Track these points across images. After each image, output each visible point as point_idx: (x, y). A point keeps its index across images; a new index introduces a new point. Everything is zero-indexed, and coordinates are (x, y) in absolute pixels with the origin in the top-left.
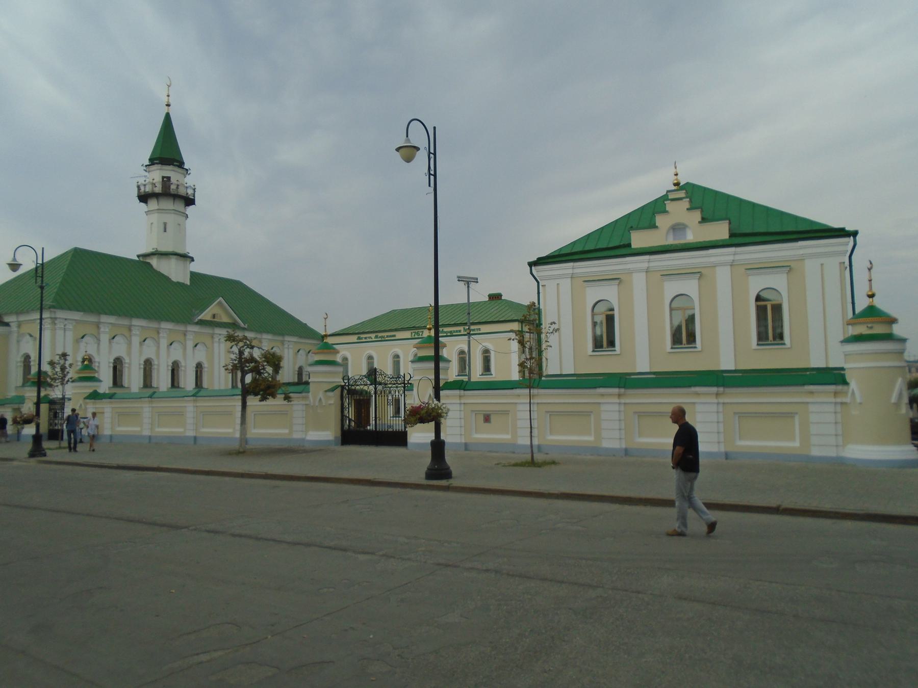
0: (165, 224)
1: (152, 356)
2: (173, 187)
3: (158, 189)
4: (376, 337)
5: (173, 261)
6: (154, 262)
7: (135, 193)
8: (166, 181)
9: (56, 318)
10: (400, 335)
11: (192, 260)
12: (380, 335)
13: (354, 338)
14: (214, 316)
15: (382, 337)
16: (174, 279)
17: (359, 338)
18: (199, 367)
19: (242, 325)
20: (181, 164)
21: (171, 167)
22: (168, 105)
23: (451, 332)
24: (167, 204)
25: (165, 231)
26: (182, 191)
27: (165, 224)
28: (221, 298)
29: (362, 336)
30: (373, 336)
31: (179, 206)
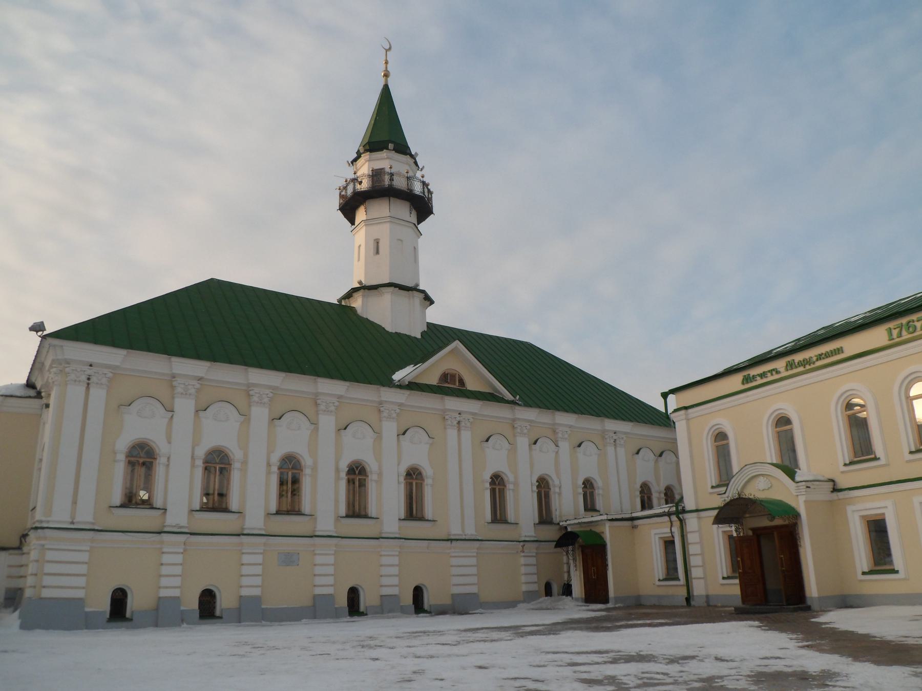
0: (377, 242)
1: (299, 448)
2: (387, 178)
3: (365, 185)
4: (790, 366)
5: (387, 298)
6: (357, 303)
7: (336, 202)
8: (376, 175)
9: (68, 362)
10: (852, 344)
11: (429, 300)
13: (735, 383)
14: (445, 377)
16: (389, 328)
18: (413, 476)
19: (509, 396)
20: (402, 148)
21: (384, 154)
22: (386, 75)
24: (381, 209)
25: (377, 252)
26: (400, 183)
27: (377, 242)
28: (457, 342)
29: (754, 372)
30: (780, 364)
31: (404, 211)
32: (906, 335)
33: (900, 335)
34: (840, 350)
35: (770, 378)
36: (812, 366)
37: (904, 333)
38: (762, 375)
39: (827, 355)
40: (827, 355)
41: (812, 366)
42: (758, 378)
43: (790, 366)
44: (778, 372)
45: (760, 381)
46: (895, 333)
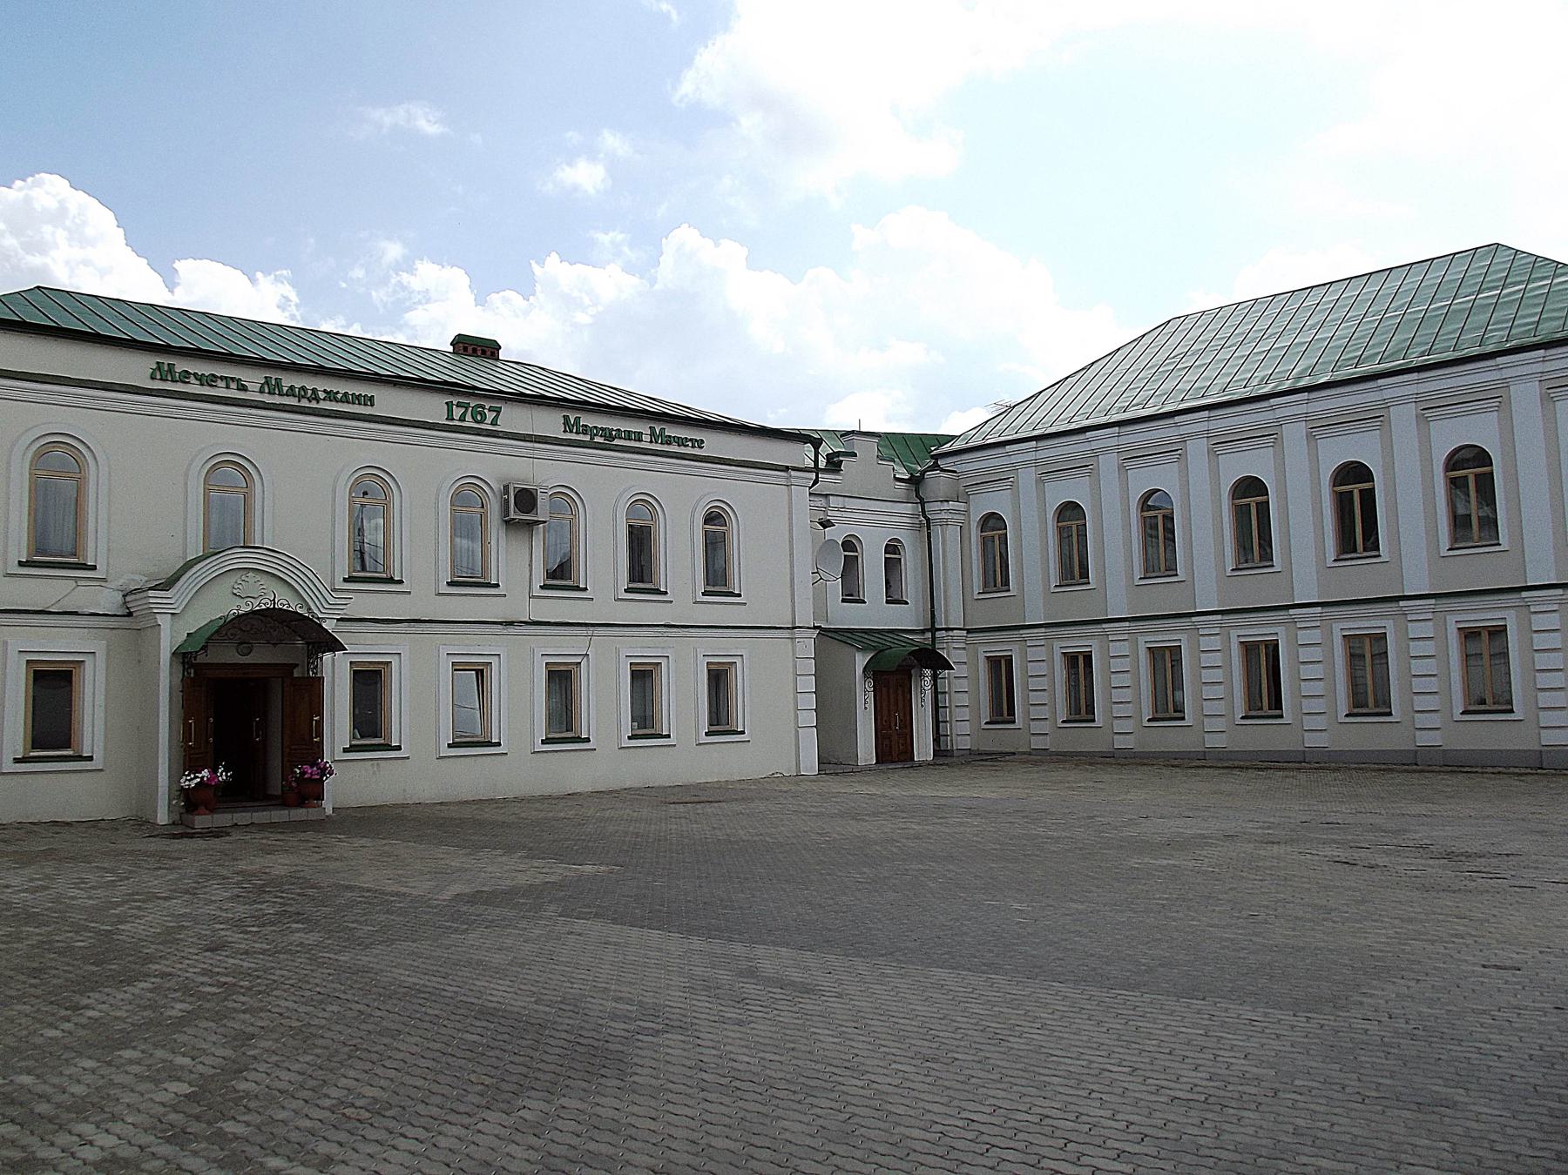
4: (272, 387)
10: (389, 402)
12: (288, 381)
13: (138, 368)
15: (302, 393)
17: (161, 373)
23: (608, 434)
32: (469, 423)
33: (462, 419)
34: (370, 401)
35: (221, 392)
36: (314, 405)
37: (469, 417)
38: (211, 380)
39: (345, 399)
40: (345, 399)
41: (314, 405)
42: (192, 380)
43: (272, 387)
44: (243, 388)
45: (194, 388)
46: (457, 412)
